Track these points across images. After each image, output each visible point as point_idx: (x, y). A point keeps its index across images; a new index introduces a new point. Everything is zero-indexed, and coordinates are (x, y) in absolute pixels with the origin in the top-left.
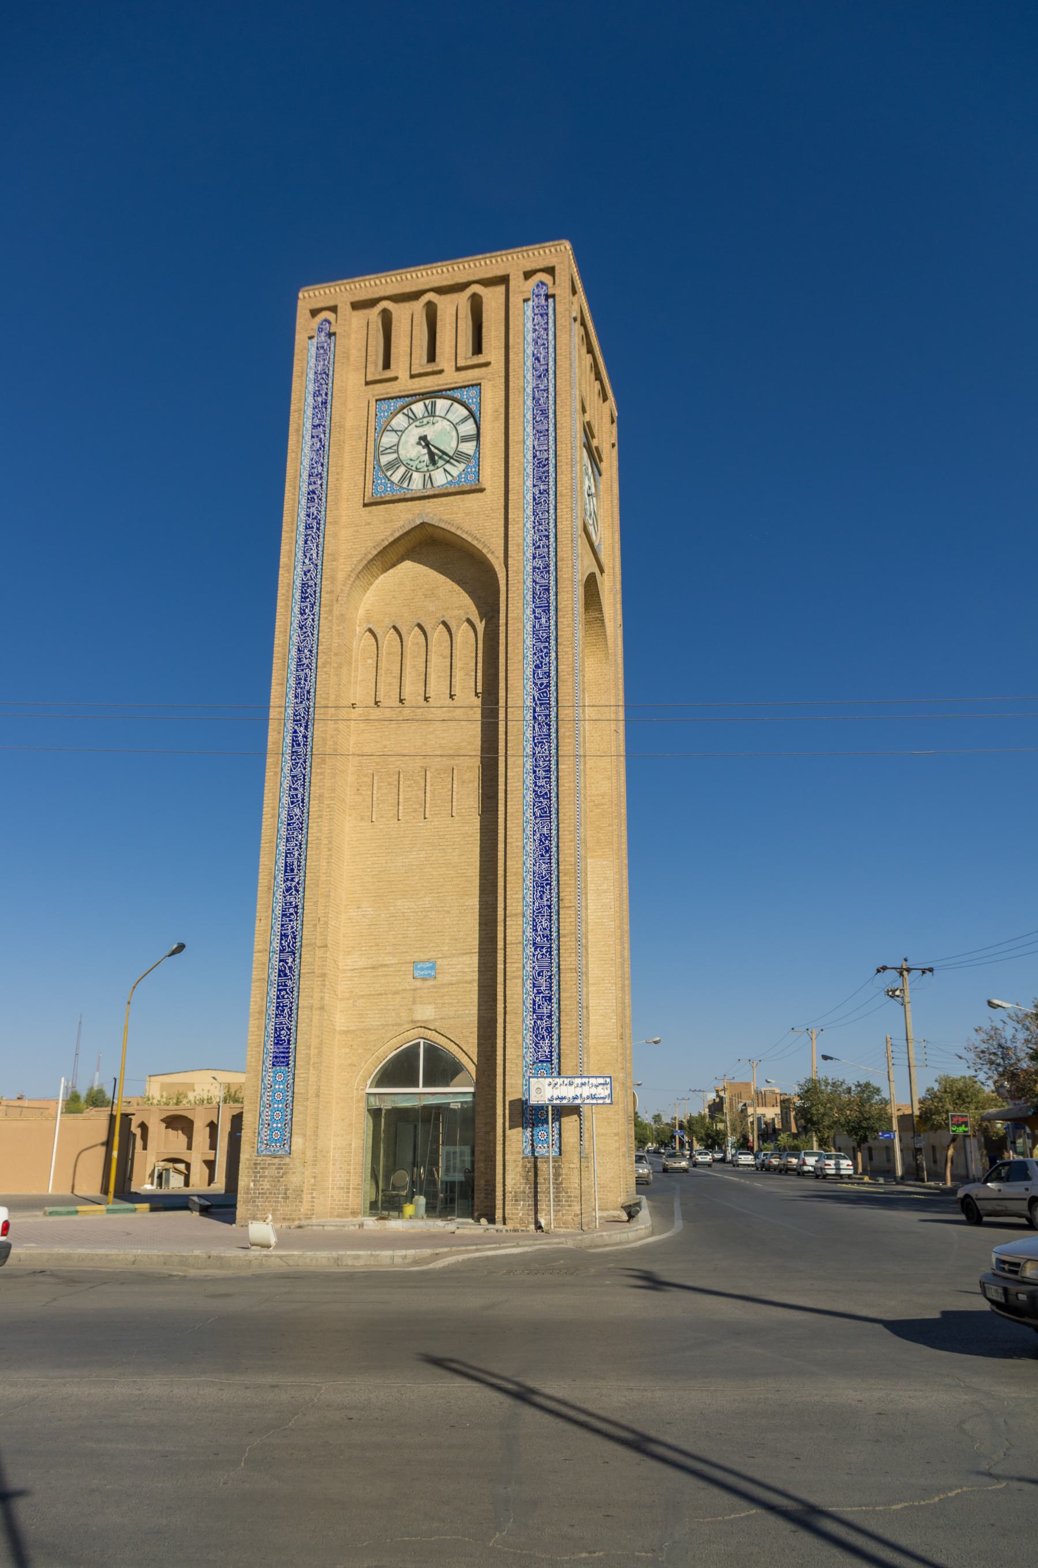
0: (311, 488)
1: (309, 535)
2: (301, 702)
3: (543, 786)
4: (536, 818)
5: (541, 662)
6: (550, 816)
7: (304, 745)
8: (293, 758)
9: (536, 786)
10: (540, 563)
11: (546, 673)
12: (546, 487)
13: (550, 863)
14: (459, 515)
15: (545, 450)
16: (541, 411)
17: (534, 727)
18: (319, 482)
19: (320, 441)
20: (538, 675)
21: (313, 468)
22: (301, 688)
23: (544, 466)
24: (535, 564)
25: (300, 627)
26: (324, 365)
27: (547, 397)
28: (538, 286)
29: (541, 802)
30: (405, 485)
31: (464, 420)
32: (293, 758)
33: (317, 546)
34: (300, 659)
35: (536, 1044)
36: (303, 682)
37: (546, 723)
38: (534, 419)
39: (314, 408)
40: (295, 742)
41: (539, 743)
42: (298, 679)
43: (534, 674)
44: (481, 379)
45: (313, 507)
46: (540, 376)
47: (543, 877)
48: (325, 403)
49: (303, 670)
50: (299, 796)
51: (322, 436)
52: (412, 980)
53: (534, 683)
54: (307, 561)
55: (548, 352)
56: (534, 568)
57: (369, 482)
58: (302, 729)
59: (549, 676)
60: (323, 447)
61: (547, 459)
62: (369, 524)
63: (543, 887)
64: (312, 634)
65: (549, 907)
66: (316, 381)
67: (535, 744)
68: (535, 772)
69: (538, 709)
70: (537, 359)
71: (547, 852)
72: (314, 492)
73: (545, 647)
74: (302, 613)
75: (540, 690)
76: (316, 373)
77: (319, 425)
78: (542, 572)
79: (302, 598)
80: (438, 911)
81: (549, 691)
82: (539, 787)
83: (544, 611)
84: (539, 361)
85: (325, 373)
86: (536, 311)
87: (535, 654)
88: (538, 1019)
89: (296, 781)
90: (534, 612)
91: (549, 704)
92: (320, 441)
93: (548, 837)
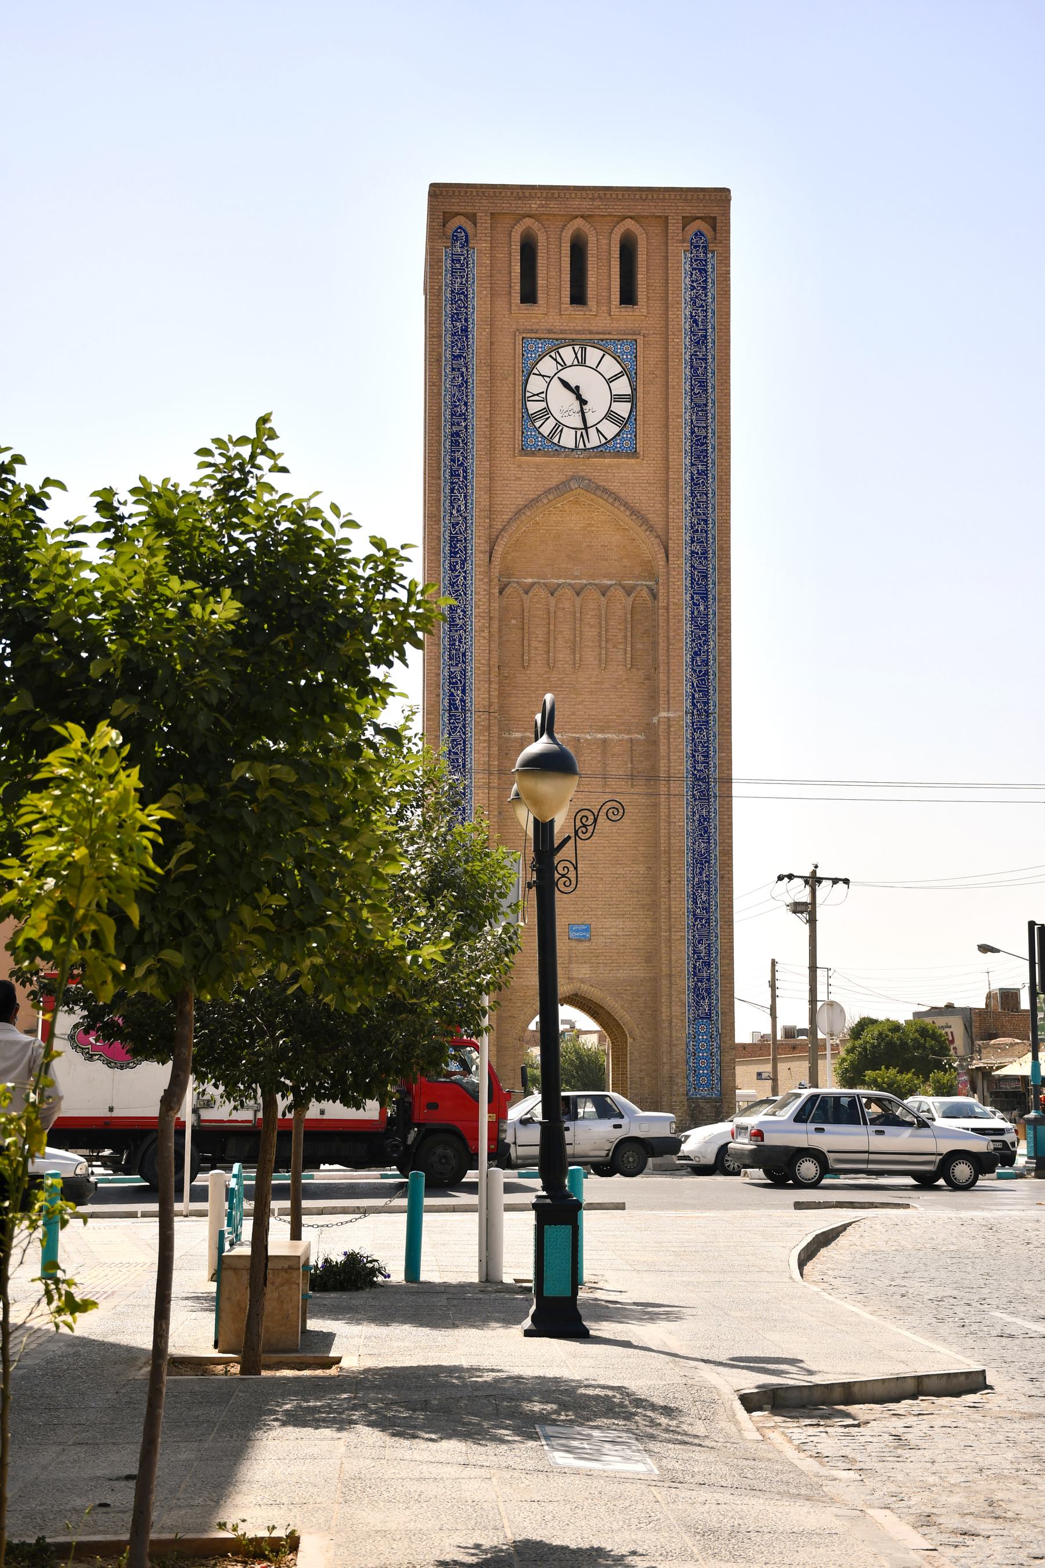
0: (455, 429)
1: (455, 483)
2: (457, 665)
3: (702, 771)
4: (695, 800)
5: (700, 650)
6: (708, 799)
7: (462, 709)
8: (452, 721)
9: (695, 769)
10: (698, 548)
11: (704, 661)
12: (704, 468)
13: (709, 842)
14: (614, 484)
15: (704, 427)
16: (699, 382)
17: (693, 712)
18: (463, 424)
19: (462, 376)
20: (696, 662)
21: (456, 406)
22: (456, 650)
23: (703, 444)
24: (693, 548)
25: (450, 584)
26: (461, 284)
27: (705, 368)
28: (696, 234)
29: (700, 785)
30: (556, 440)
32: (452, 721)
33: (465, 497)
34: (453, 618)
35: (697, 1003)
36: (457, 643)
37: (705, 710)
38: (692, 390)
39: (452, 335)
40: (452, 703)
41: (698, 729)
42: (452, 641)
43: (693, 661)
45: (459, 451)
46: (698, 343)
47: (702, 855)
48: (465, 330)
49: (456, 631)
50: (460, 760)
51: (464, 370)
52: (568, 941)
53: (693, 669)
54: (454, 512)
55: (706, 316)
56: (692, 552)
57: (518, 433)
58: (459, 692)
59: (707, 665)
60: (466, 382)
61: (706, 437)
62: (519, 479)
63: (702, 864)
64: (465, 594)
65: (708, 882)
66: (453, 301)
67: (694, 729)
68: (694, 756)
69: (696, 696)
70: (695, 321)
71: (706, 832)
72: (457, 434)
73: (703, 635)
74: (453, 569)
75: (698, 677)
76: (452, 292)
77: (460, 356)
78: (700, 558)
79: (451, 552)
80: (591, 878)
81: (708, 679)
82: (698, 771)
83: (702, 598)
84: (697, 325)
85: (463, 293)
86: (695, 266)
87: (693, 640)
88: (698, 981)
89: (456, 746)
90: (692, 598)
91: (707, 691)
92: (462, 376)
93: (707, 819)
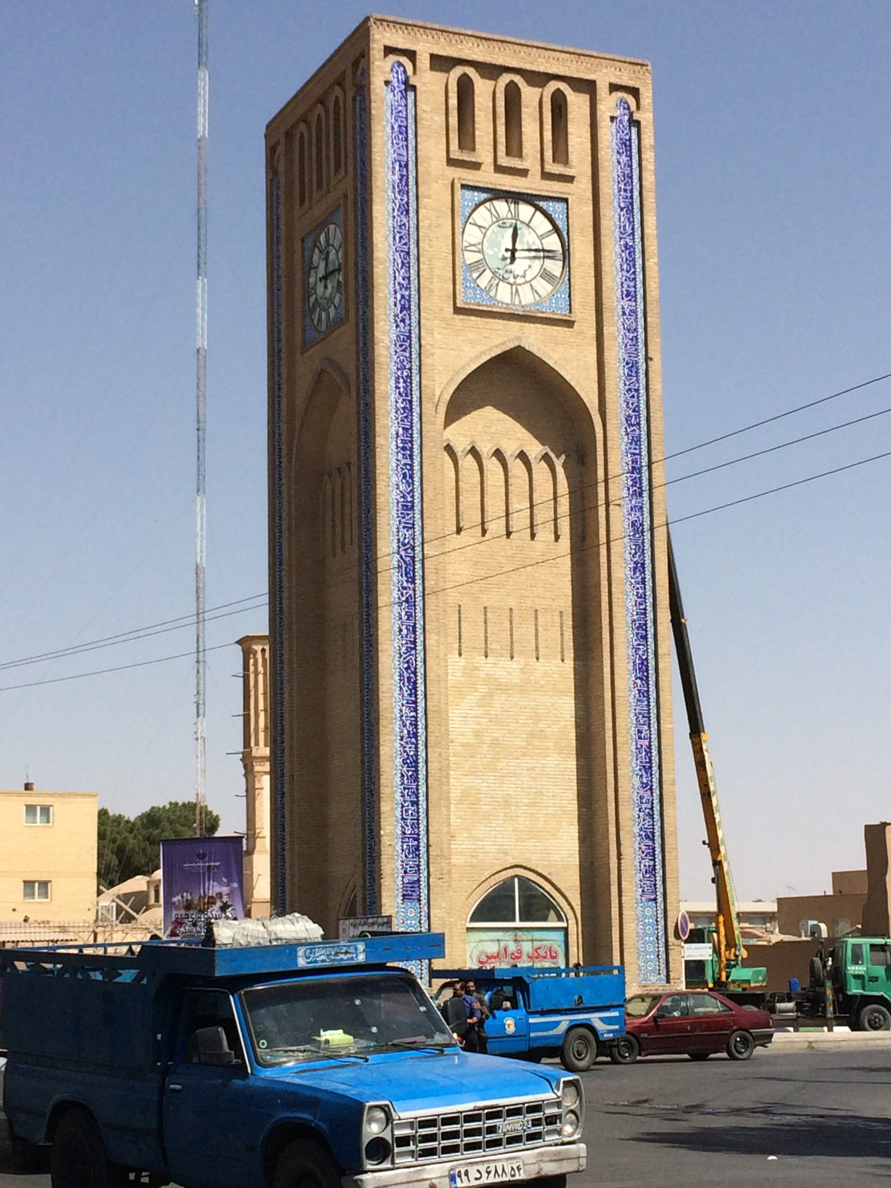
30: (492, 294)
31: (547, 234)
44: (569, 194)
